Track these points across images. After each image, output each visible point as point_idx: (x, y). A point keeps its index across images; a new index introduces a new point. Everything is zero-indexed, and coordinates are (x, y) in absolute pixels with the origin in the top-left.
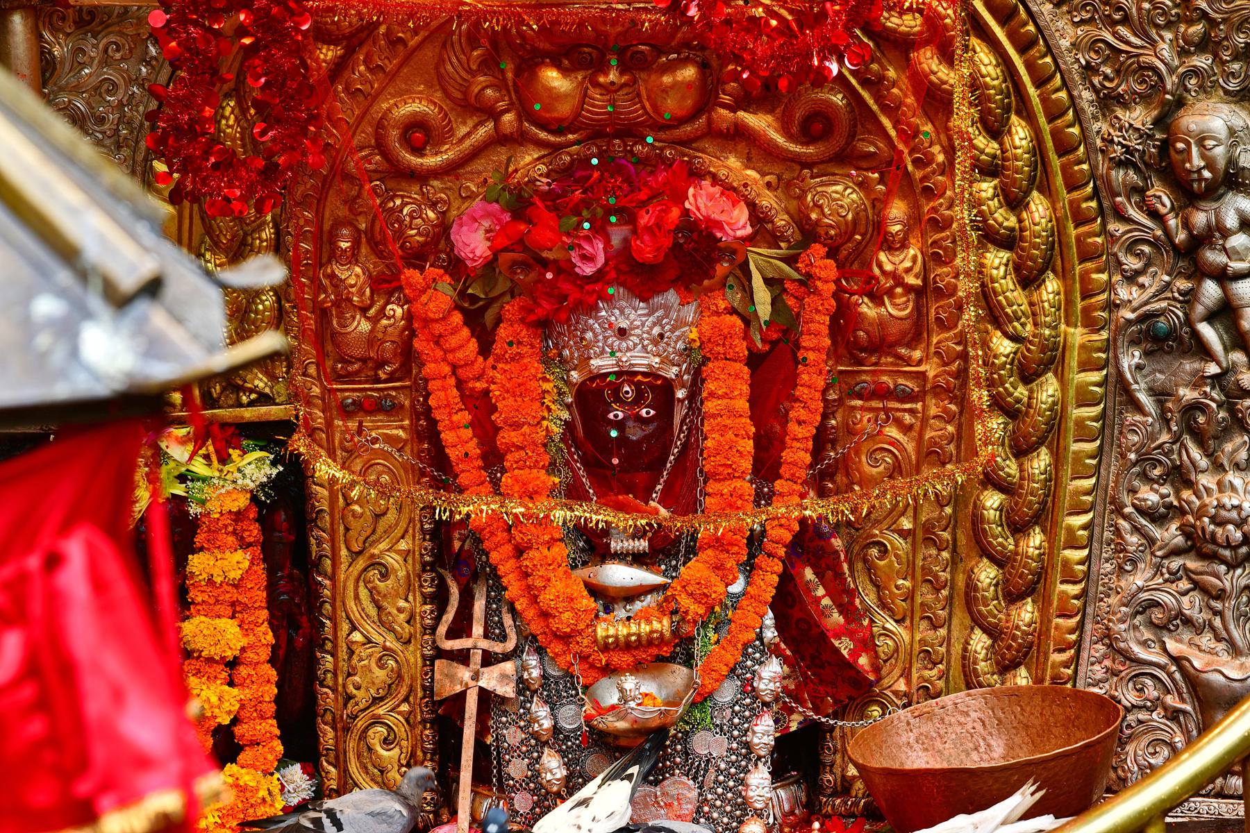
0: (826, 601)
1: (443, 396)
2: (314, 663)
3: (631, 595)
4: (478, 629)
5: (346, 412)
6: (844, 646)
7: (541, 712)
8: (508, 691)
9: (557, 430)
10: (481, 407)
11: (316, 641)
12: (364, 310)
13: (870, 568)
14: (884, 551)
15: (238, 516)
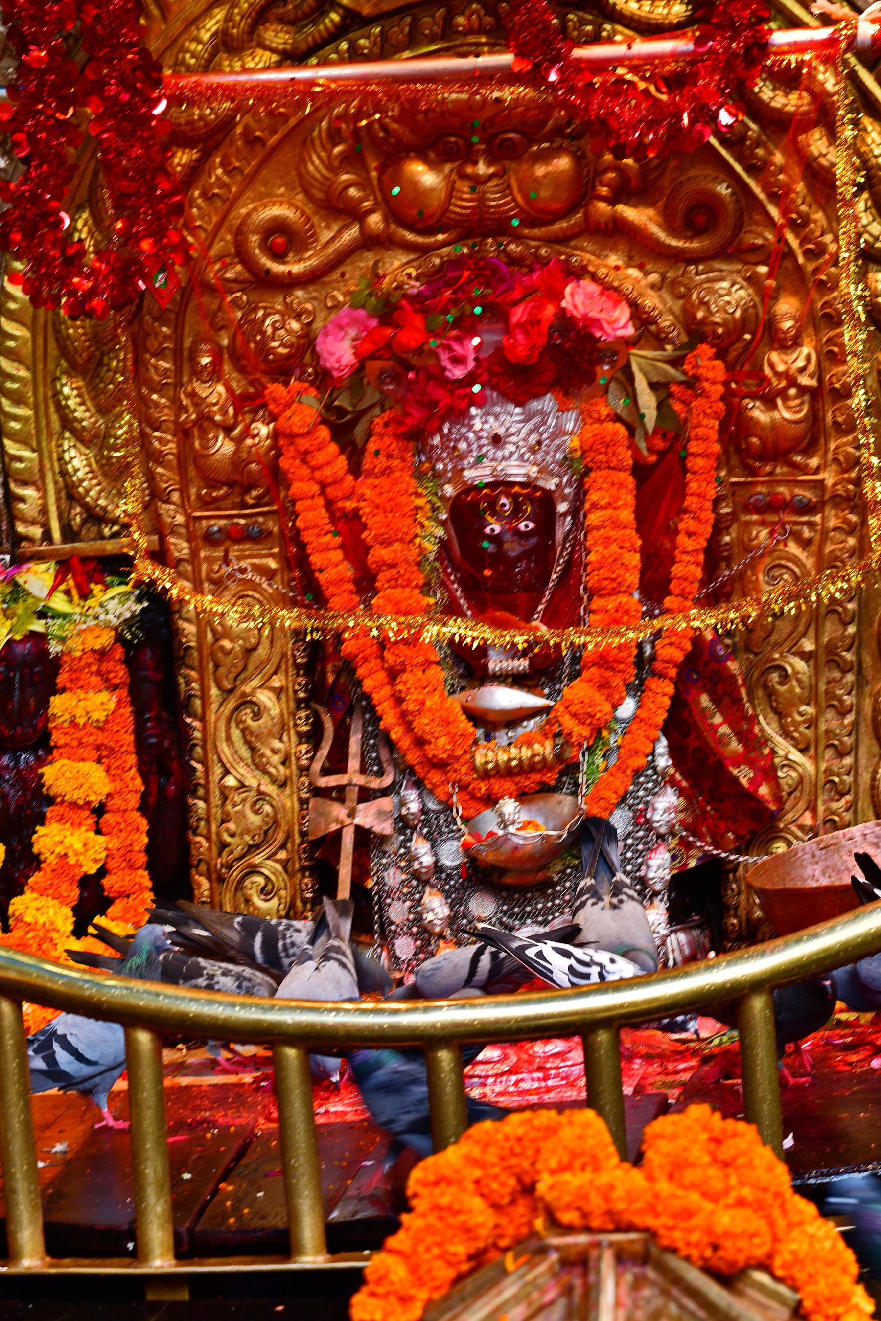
0: (724, 729)
1: (312, 515)
2: (186, 810)
3: (513, 719)
4: (354, 764)
5: (210, 539)
6: (744, 775)
7: (421, 848)
8: (385, 827)
9: (431, 547)
10: (349, 526)
11: (188, 786)
12: (228, 430)
13: (770, 693)
14: (785, 678)
15: (102, 654)
